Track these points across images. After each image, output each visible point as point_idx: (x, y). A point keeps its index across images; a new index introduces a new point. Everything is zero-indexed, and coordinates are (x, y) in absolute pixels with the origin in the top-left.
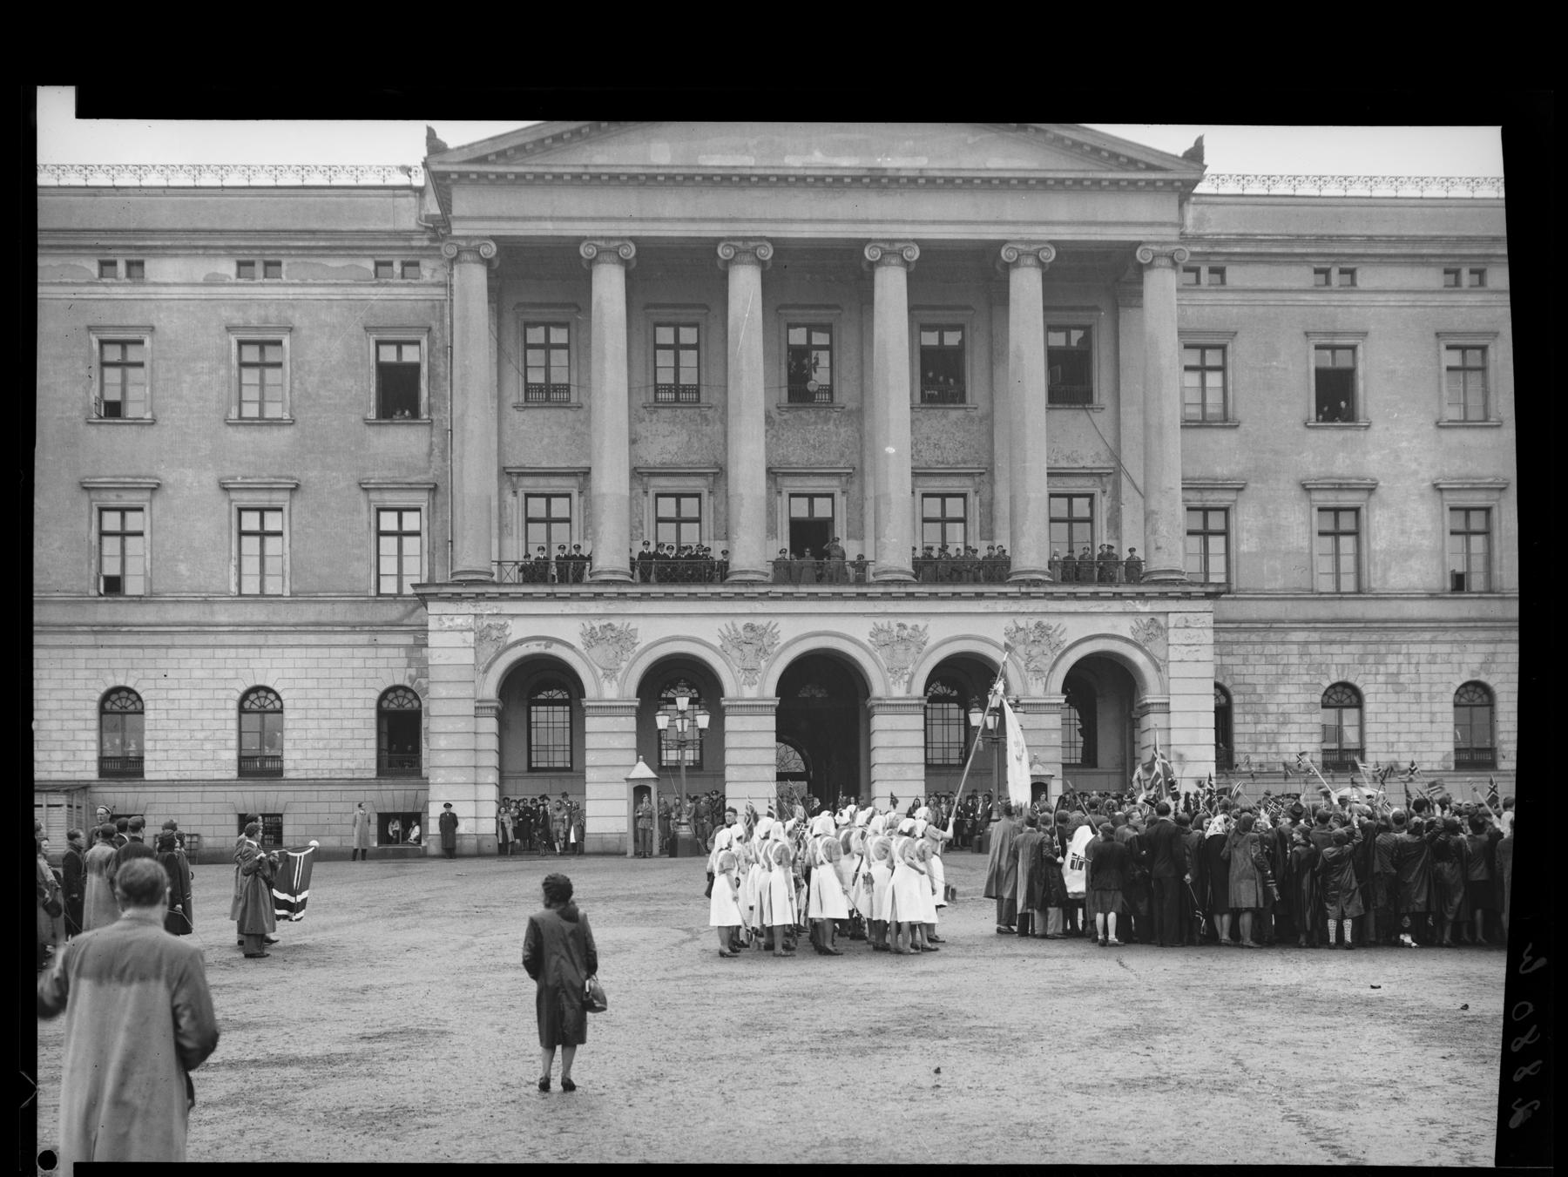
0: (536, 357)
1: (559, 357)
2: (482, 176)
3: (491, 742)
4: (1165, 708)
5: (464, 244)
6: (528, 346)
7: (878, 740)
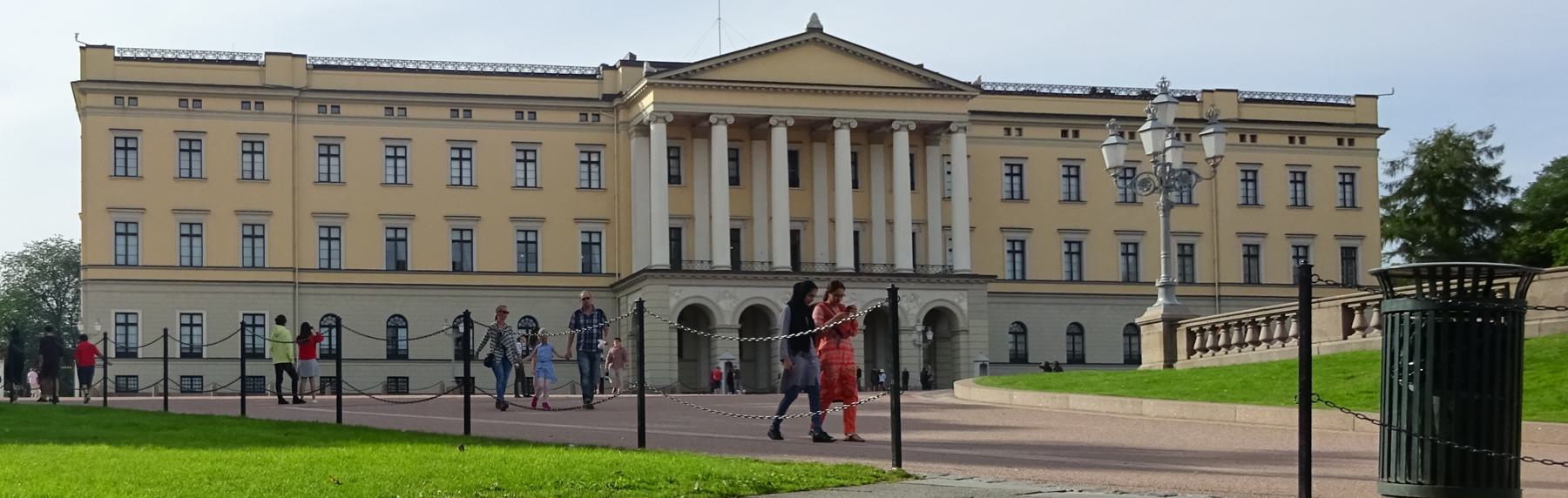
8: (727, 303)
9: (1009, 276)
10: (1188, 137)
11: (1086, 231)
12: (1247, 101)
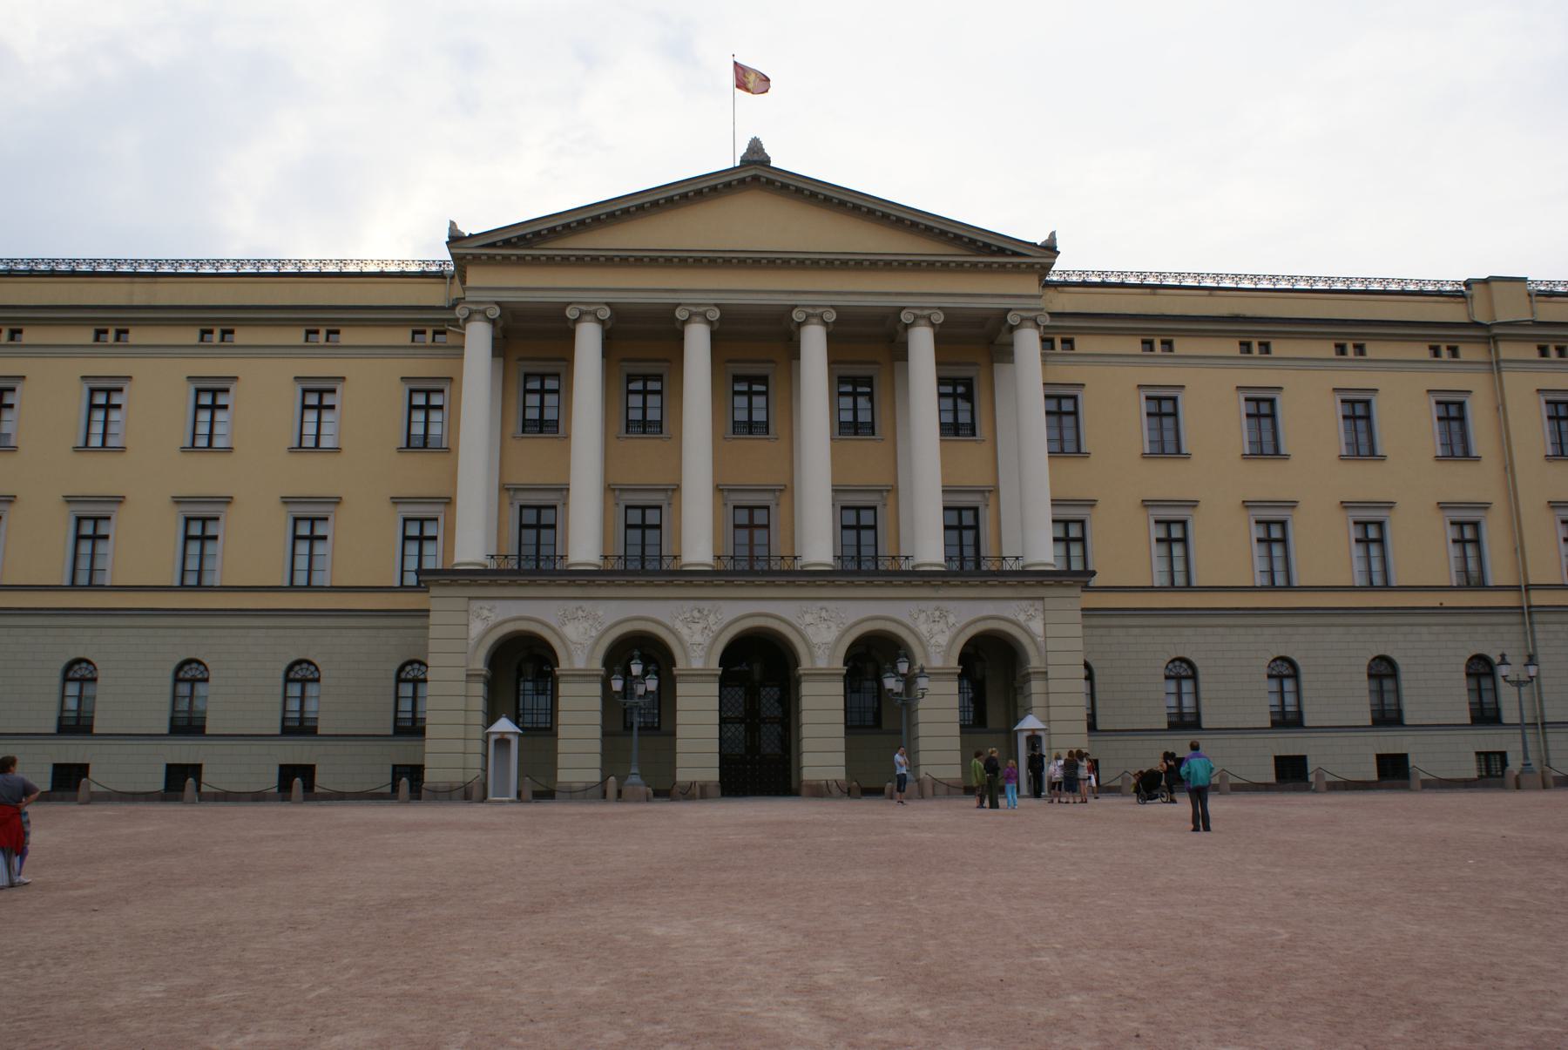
0: (533, 400)
1: (550, 400)
2: (491, 258)
3: (479, 704)
4: (1044, 675)
5: (474, 307)
6: (527, 391)
7: (806, 703)
8: (580, 631)
9: (1165, 581)
10: (1454, 351)
11: (1292, 505)
12: (1541, 294)
